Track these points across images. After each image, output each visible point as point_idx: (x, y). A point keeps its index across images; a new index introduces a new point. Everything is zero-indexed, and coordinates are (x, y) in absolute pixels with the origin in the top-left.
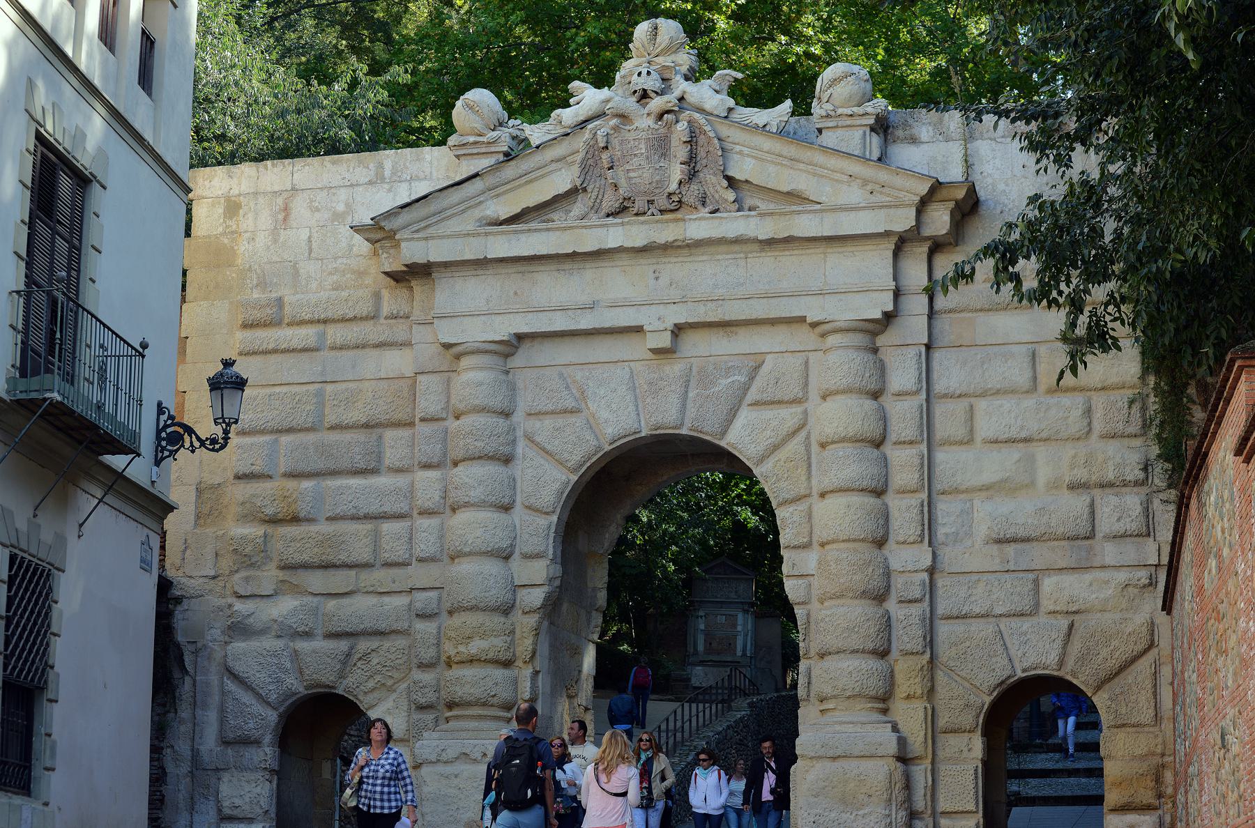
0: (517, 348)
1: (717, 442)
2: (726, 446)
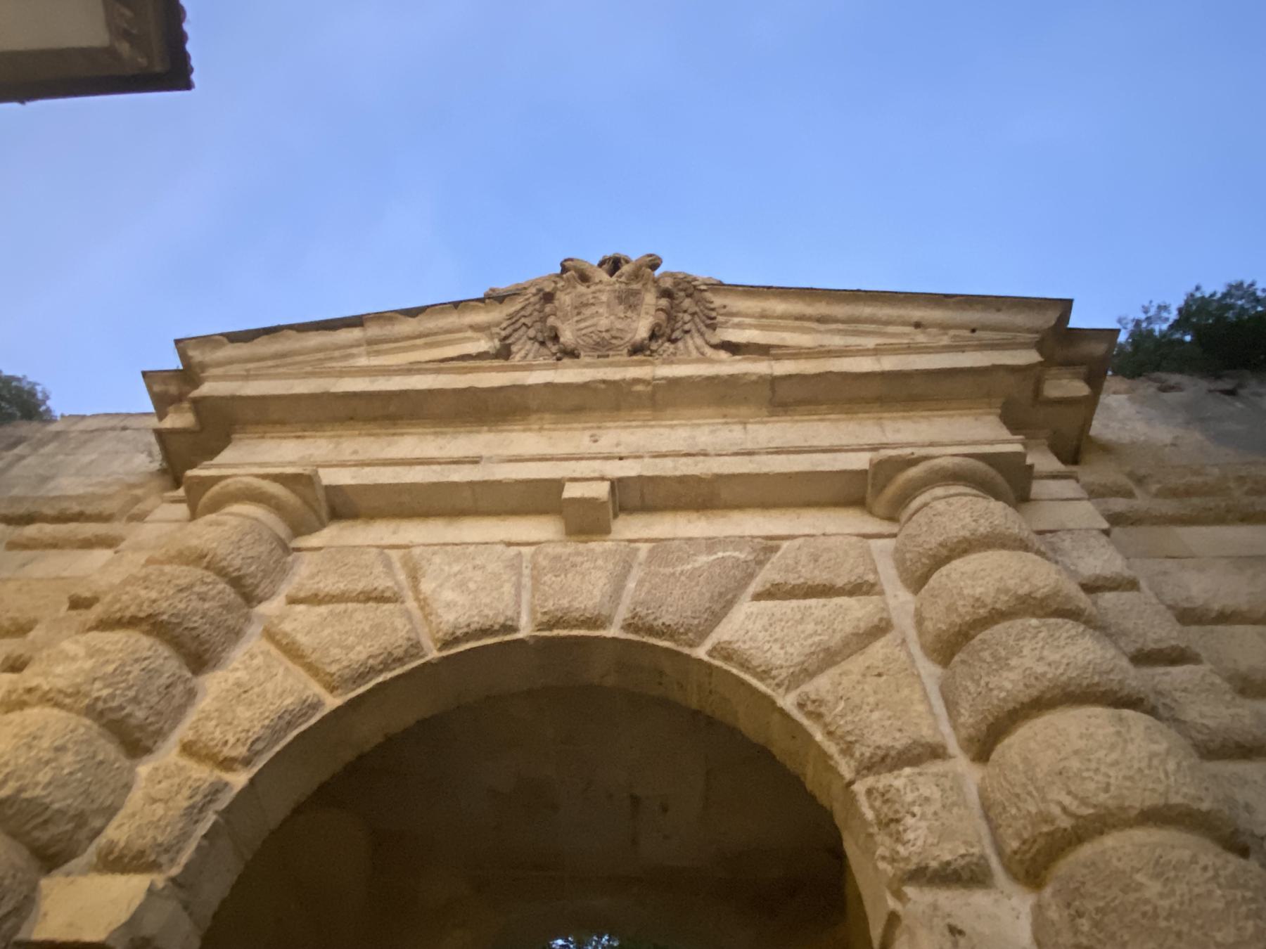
0: (323, 525)
1: (686, 650)
2: (706, 658)
